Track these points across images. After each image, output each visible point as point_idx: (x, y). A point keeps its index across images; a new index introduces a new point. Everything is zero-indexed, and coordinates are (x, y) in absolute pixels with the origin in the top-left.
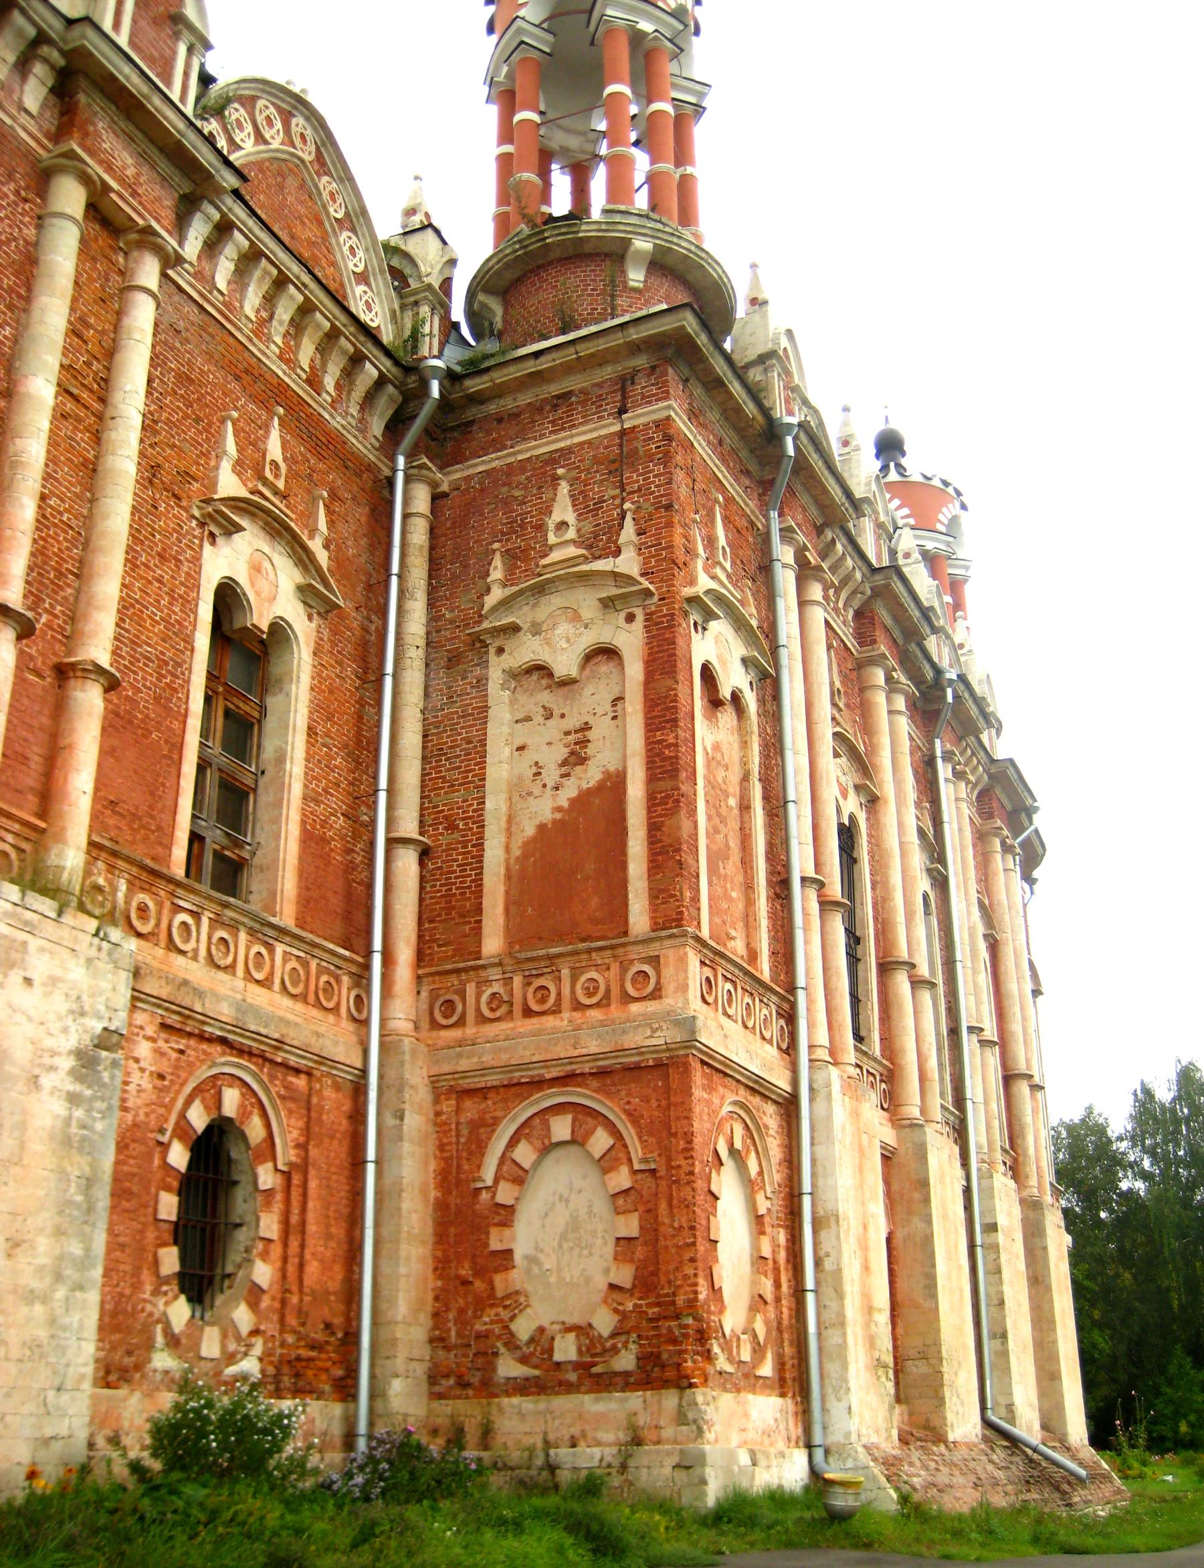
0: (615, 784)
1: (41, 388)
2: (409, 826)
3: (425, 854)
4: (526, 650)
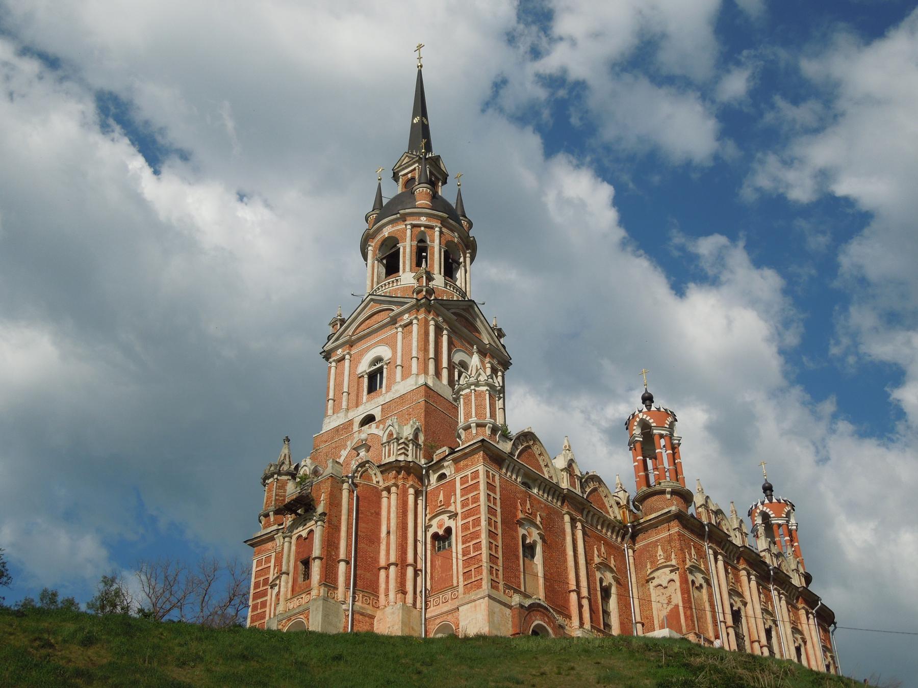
0: (677, 606)
2: (638, 619)
3: (643, 625)
4: (655, 582)
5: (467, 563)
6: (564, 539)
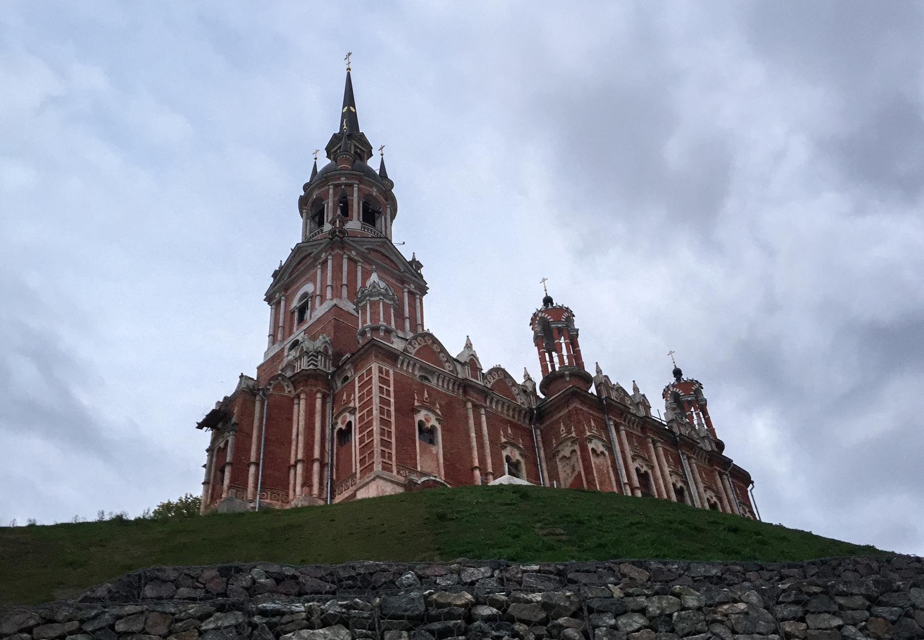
0: (580, 473)
1: (473, 435)
5: (362, 450)
6: (467, 423)
